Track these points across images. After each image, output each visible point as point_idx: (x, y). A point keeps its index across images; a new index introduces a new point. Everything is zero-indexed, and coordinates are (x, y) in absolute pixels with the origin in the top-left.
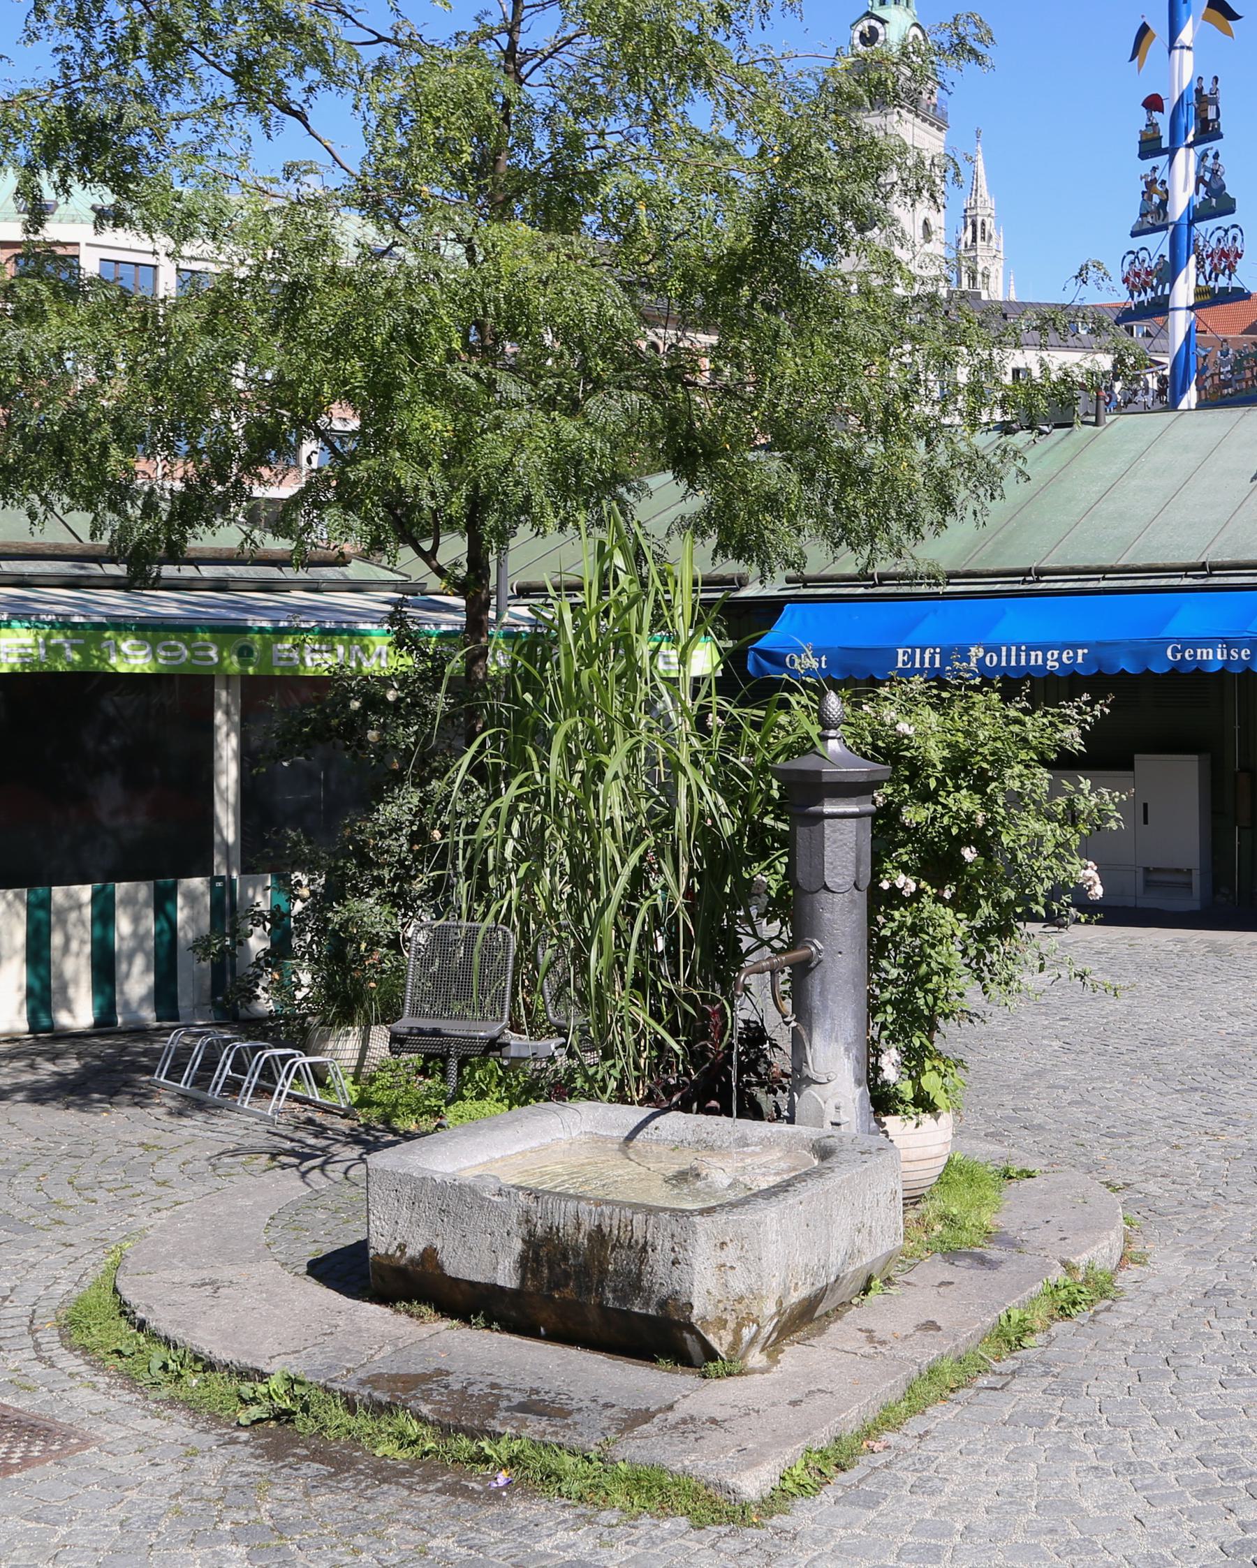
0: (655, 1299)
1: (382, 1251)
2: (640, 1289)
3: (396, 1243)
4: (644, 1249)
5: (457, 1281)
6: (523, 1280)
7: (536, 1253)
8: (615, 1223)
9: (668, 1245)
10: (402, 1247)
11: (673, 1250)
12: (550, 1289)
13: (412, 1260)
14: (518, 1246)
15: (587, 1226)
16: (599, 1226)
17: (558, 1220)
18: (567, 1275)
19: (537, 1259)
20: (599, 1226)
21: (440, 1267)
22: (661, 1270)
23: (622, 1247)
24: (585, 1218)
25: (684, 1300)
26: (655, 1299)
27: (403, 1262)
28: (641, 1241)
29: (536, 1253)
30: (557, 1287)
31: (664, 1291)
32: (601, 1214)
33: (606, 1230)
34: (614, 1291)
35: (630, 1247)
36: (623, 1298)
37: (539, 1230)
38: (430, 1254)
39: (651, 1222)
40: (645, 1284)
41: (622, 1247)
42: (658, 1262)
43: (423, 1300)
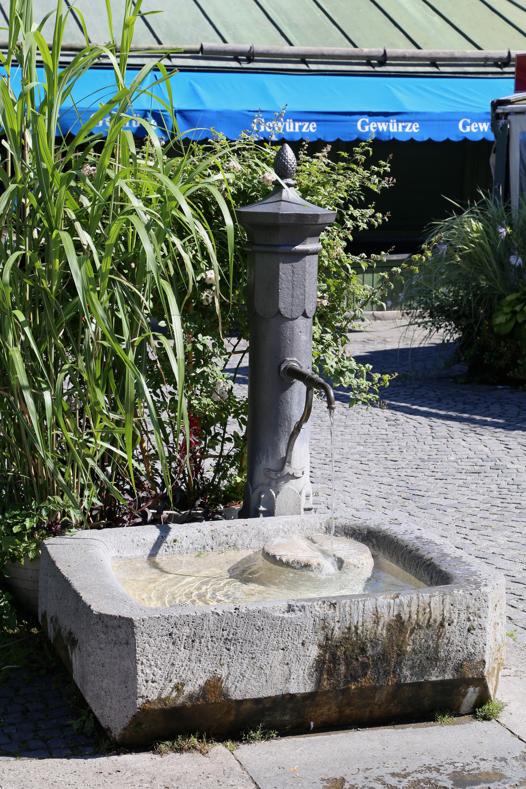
0: (451, 665)
1: (153, 697)
2: (437, 659)
3: (172, 685)
4: (442, 625)
5: (240, 703)
6: (319, 682)
7: (334, 655)
8: (414, 609)
9: (463, 616)
10: (178, 688)
11: (469, 620)
12: (347, 682)
13: (191, 697)
14: (314, 652)
15: (387, 617)
16: (399, 616)
17: (357, 618)
18: (365, 666)
19: (334, 659)
20: (399, 616)
21: (226, 695)
22: (456, 639)
23: (420, 627)
24: (383, 611)
25: (478, 659)
26: (451, 665)
27: (180, 700)
28: (439, 619)
29: (334, 655)
30: (355, 678)
31: (461, 656)
32: (401, 605)
33: (405, 617)
34: (412, 668)
35: (429, 626)
36: (423, 671)
37: (337, 633)
38: (213, 686)
39: (448, 600)
40: (442, 654)
41: (420, 627)
42: (454, 633)
43: (187, 733)
